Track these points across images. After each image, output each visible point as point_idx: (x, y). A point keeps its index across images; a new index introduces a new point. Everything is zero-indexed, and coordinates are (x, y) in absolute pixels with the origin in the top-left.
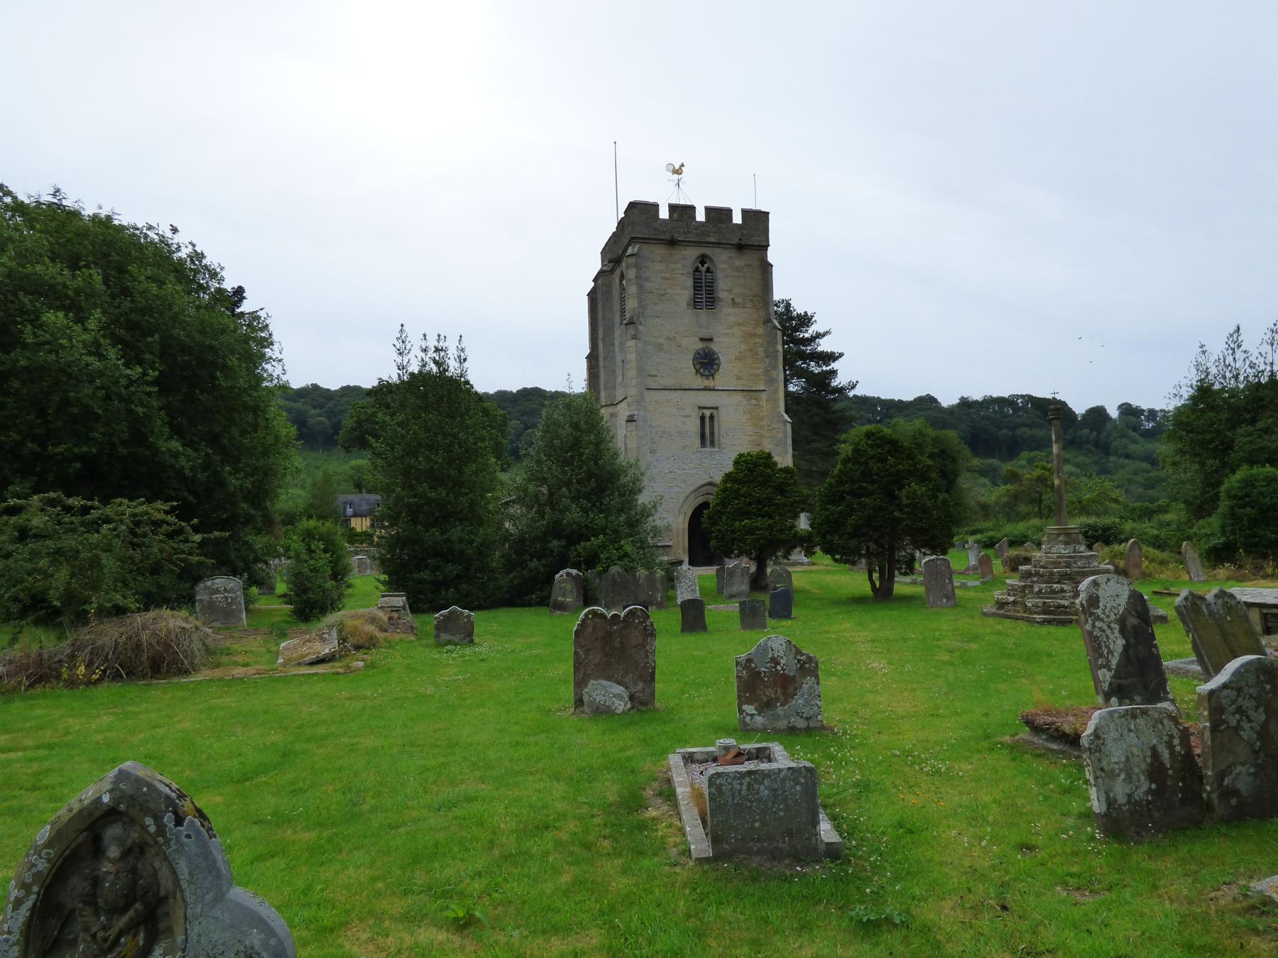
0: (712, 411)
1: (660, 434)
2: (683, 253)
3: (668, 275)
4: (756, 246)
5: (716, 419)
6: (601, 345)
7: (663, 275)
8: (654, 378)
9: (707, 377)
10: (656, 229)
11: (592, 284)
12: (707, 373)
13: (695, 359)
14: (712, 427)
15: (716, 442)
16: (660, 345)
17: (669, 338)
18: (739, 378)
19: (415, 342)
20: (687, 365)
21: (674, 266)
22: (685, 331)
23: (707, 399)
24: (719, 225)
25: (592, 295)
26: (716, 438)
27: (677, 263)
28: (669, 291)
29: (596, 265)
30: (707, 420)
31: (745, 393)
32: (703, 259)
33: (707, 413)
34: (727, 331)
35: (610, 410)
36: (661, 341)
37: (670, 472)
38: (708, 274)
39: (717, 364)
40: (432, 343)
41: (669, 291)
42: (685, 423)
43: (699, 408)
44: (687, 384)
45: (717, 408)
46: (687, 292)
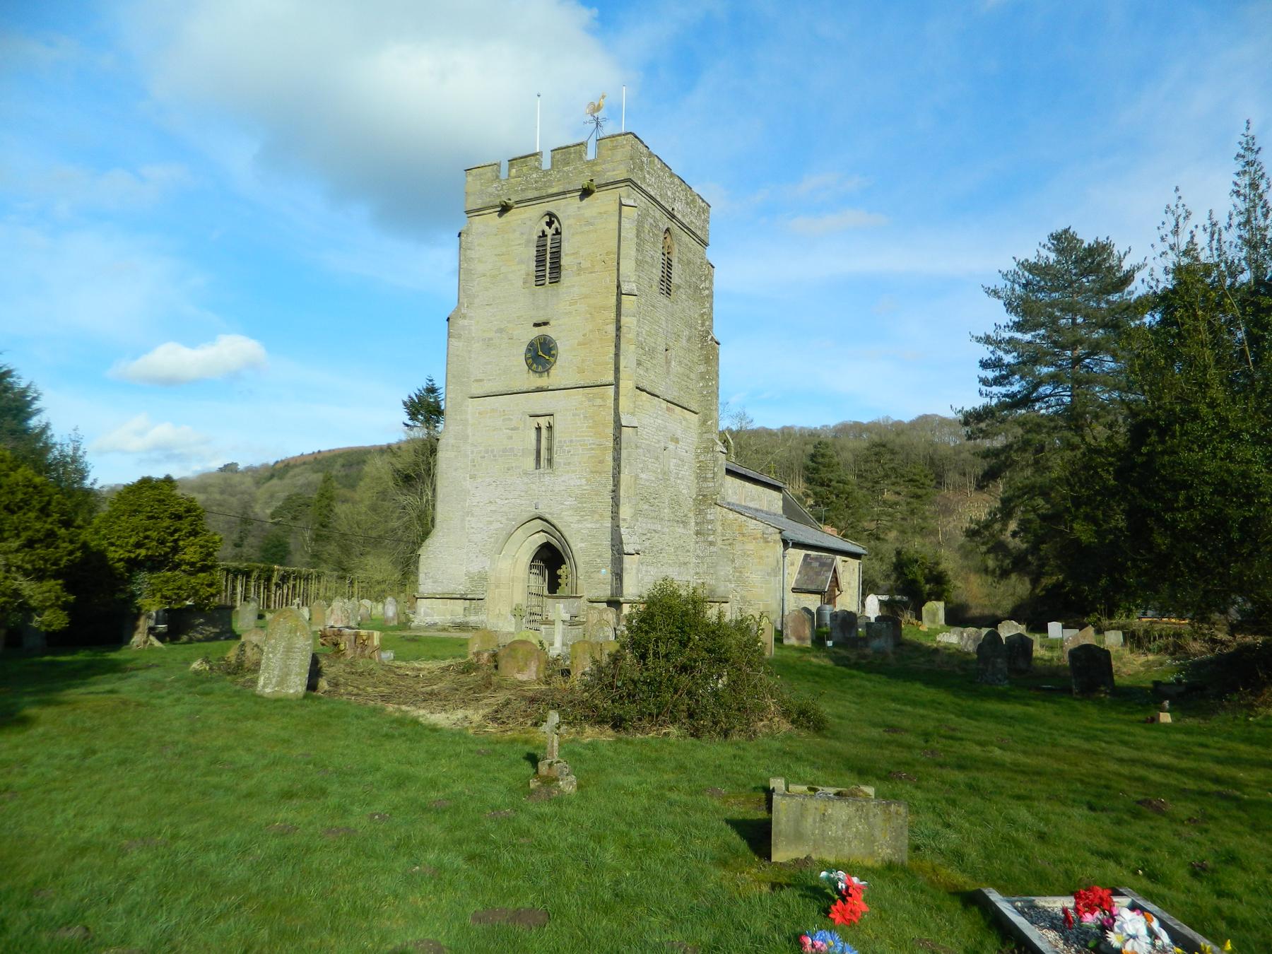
1: (482, 454)
4: (612, 183)
8: (481, 383)
9: (541, 373)
12: (540, 368)
13: (528, 350)
14: (550, 439)
17: (500, 331)
18: (581, 371)
22: (518, 318)
30: (544, 432)
32: (551, 218)
37: (491, 502)
42: (511, 438)
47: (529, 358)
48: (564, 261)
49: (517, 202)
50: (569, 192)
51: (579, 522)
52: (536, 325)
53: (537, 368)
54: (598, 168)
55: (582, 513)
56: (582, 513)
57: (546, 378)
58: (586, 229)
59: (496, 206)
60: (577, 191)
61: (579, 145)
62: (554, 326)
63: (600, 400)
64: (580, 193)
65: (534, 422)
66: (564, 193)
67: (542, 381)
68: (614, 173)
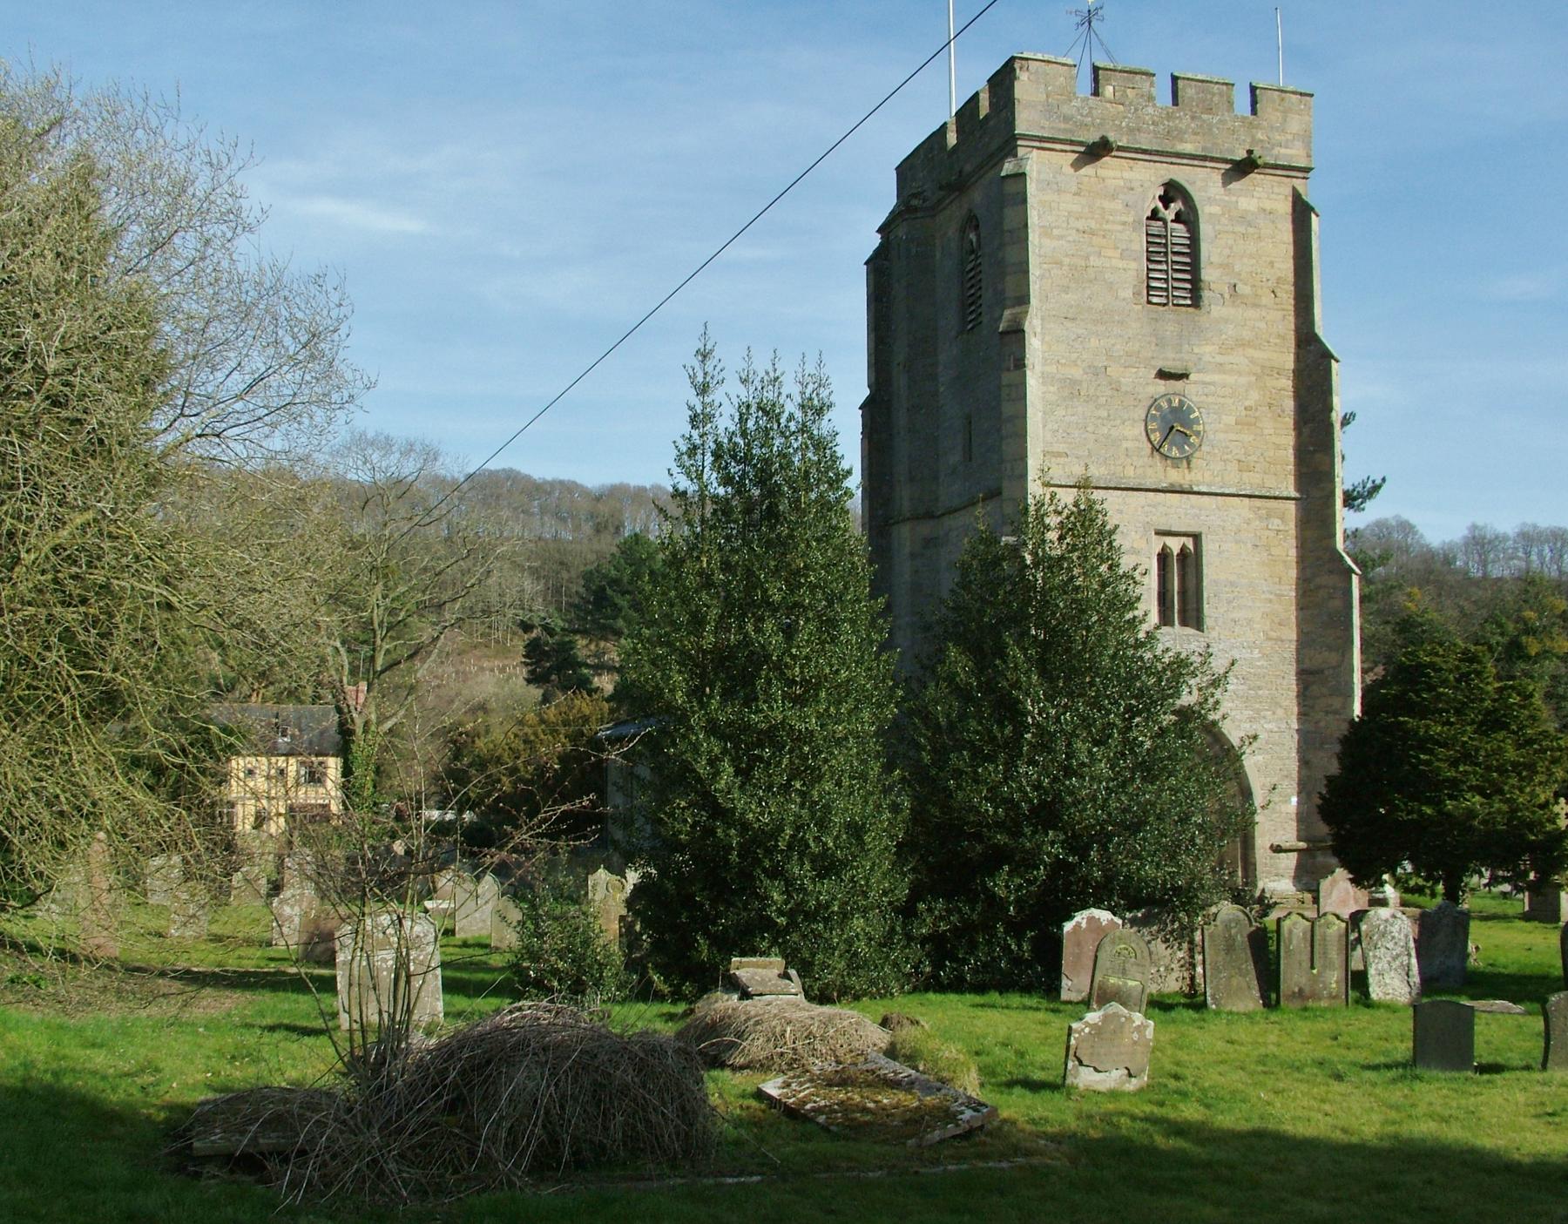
0: (1184, 540)
2: (1126, 175)
3: (1093, 225)
5: (1191, 561)
6: (900, 381)
7: (1080, 225)
8: (1061, 460)
9: (1176, 463)
10: (1067, 119)
11: (876, 240)
12: (1175, 452)
15: (1193, 614)
16: (1074, 382)
19: (729, 360)
20: (1132, 433)
21: (1107, 205)
22: (1129, 355)
23: (1180, 513)
24: (1205, 116)
25: (879, 266)
26: (1192, 605)
27: (1114, 197)
28: (1093, 261)
29: (885, 199)
31: (1258, 502)
32: (1172, 192)
33: (1175, 545)
34: (1219, 359)
35: (925, 529)
36: (1077, 373)
38: (1153, 223)
39: (1198, 434)
40: (761, 366)
41: (1093, 261)
43: (1159, 533)
44: (1131, 476)
45: (1197, 538)
46: (1133, 265)
47: (1154, 431)
48: (1207, 274)
49: (1120, 149)
50: (1213, 159)
51: (1251, 720)
52: (1163, 375)
53: (1170, 450)
54: (1260, 136)
55: (1257, 706)
56: (1257, 706)
57: (1186, 471)
58: (1240, 229)
59: (1080, 143)
60: (1225, 161)
61: (1226, 84)
62: (1195, 383)
63: (1279, 522)
64: (1228, 166)
65: (1157, 545)
66: (1204, 158)
67: (1175, 476)
68: (1288, 151)
